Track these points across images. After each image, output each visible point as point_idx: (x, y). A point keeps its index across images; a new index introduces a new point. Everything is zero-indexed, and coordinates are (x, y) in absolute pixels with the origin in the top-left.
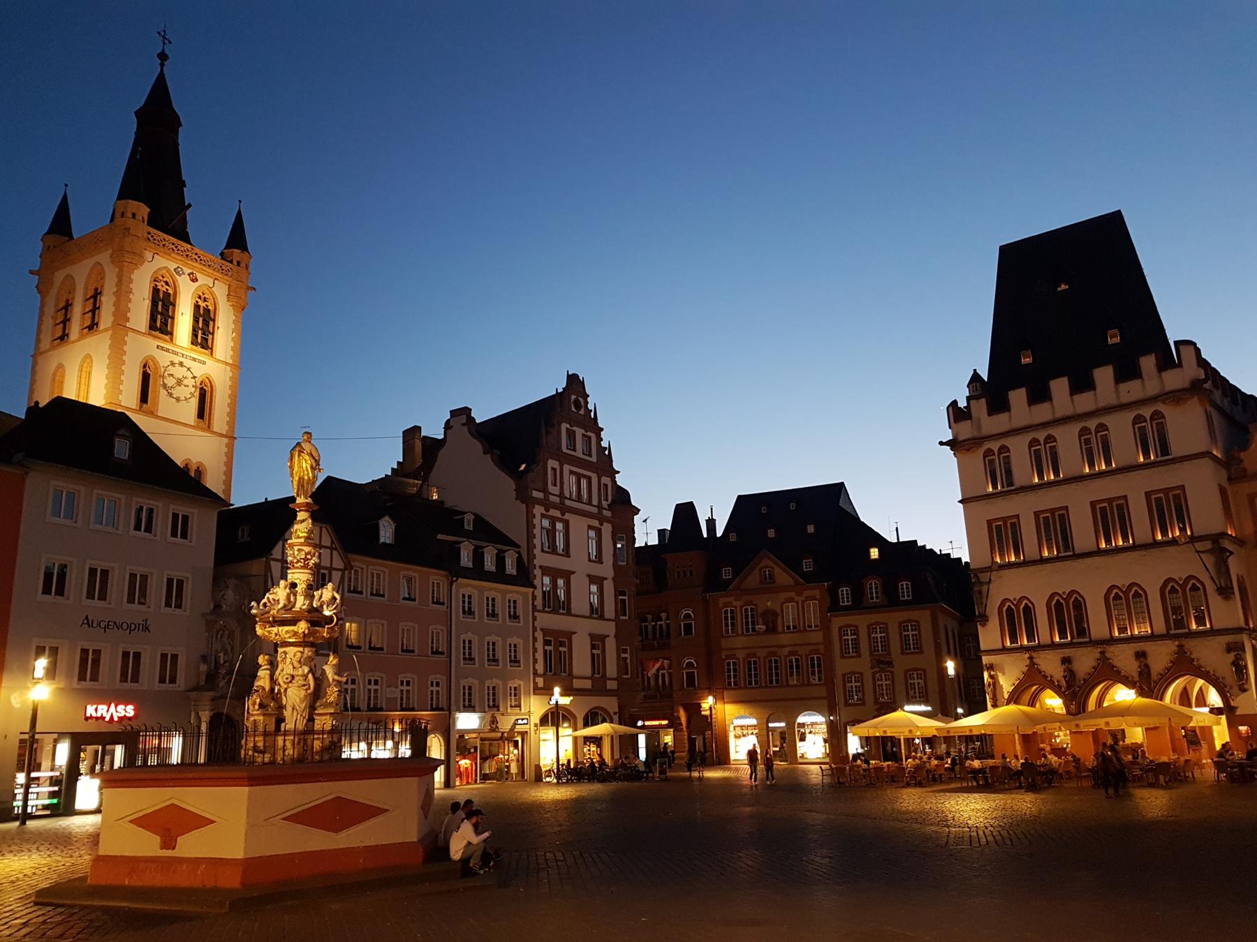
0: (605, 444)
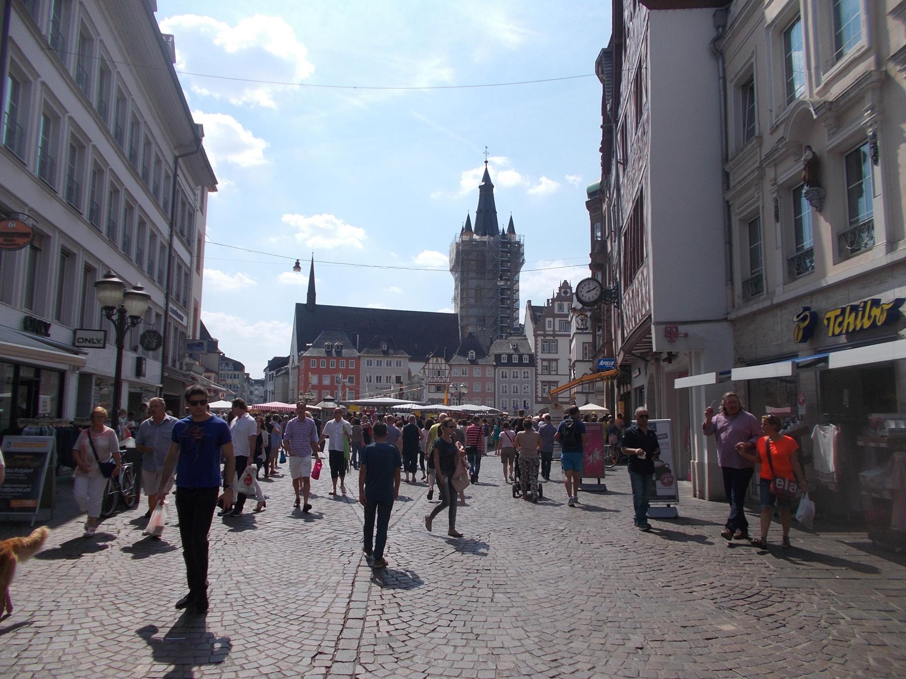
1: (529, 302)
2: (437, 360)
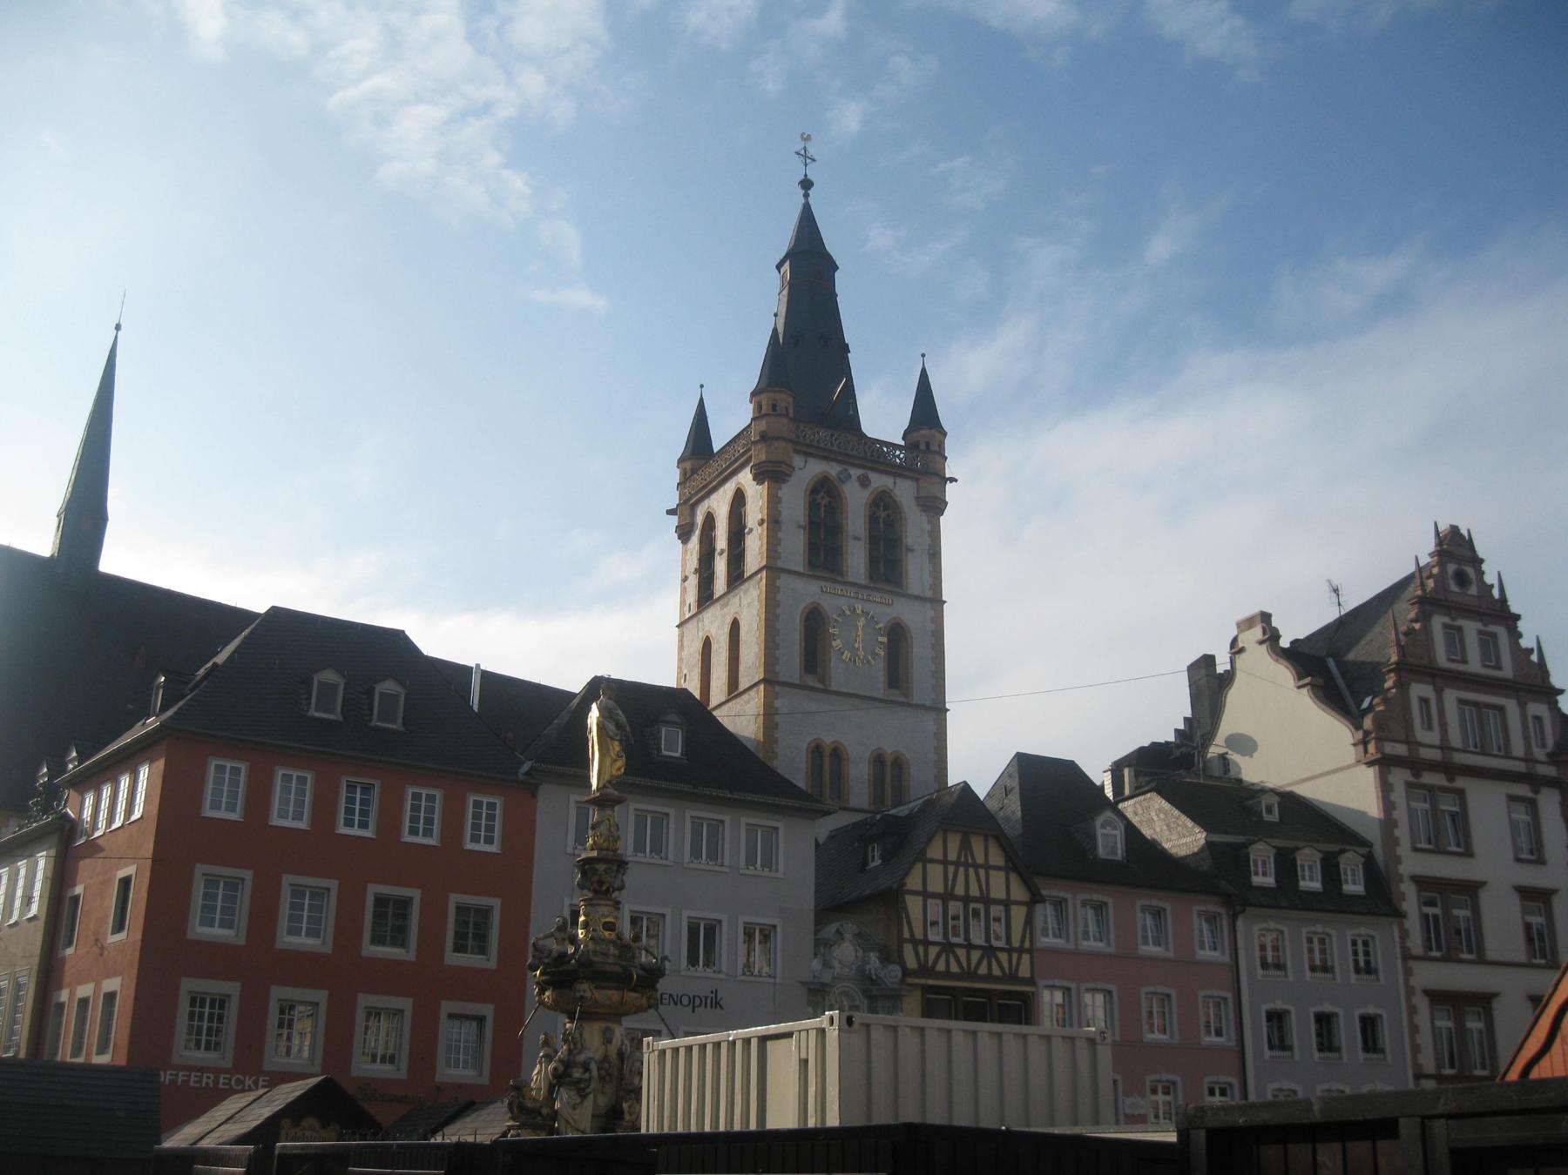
0: (1526, 642)
2: (965, 846)
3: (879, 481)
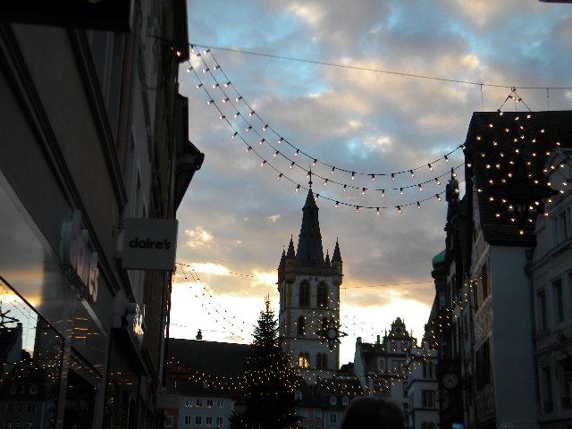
1: (359, 339)
3: (321, 279)
